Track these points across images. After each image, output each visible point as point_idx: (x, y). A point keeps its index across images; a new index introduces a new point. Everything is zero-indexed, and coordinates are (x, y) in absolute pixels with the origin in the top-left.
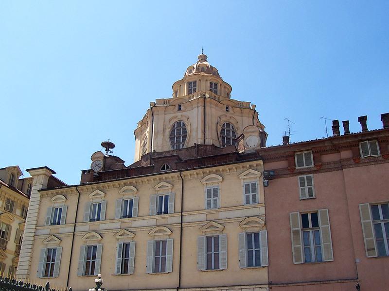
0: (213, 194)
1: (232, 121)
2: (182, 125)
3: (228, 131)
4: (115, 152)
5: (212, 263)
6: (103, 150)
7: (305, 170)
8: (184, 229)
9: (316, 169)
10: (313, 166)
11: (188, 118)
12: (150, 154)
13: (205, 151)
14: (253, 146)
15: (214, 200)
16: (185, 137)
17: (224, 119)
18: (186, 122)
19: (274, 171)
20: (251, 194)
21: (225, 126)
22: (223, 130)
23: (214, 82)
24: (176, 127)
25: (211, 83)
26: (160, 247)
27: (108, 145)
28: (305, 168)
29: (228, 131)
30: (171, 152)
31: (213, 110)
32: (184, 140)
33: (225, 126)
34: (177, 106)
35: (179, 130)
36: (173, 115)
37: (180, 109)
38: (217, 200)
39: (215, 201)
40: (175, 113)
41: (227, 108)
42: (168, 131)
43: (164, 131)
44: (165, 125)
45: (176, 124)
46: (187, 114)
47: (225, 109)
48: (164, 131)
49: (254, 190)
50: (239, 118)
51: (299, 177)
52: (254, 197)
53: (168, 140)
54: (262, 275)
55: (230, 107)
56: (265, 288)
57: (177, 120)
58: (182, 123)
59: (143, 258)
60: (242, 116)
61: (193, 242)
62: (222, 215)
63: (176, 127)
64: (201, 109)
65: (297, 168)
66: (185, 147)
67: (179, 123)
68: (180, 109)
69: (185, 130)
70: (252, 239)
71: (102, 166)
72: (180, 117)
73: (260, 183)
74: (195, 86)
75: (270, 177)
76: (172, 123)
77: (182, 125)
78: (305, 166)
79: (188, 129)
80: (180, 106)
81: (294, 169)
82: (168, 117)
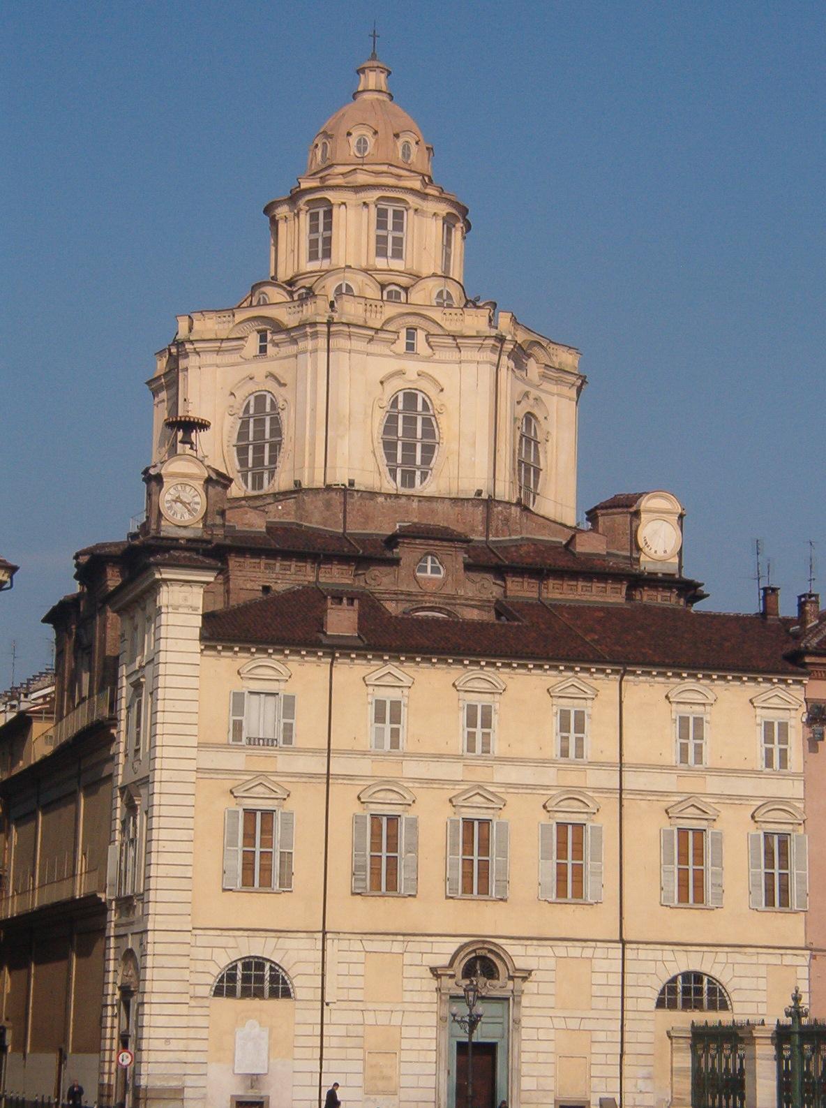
0: (691, 728)
5: (692, 889)
8: (625, 803)
13: (507, 520)
14: (660, 554)
15: (696, 745)
18: (436, 400)
20: (776, 748)
26: (569, 840)
34: (403, 333)
36: (394, 365)
37: (410, 347)
40: (398, 356)
42: (379, 419)
45: (401, 399)
49: (784, 738)
52: (783, 753)
54: (791, 928)
56: (803, 956)
57: (396, 385)
59: (526, 859)
61: (648, 835)
62: (714, 785)
64: (487, 372)
67: (410, 398)
68: (410, 347)
70: (776, 850)
71: (201, 508)
72: (412, 374)
73: (796, 720)
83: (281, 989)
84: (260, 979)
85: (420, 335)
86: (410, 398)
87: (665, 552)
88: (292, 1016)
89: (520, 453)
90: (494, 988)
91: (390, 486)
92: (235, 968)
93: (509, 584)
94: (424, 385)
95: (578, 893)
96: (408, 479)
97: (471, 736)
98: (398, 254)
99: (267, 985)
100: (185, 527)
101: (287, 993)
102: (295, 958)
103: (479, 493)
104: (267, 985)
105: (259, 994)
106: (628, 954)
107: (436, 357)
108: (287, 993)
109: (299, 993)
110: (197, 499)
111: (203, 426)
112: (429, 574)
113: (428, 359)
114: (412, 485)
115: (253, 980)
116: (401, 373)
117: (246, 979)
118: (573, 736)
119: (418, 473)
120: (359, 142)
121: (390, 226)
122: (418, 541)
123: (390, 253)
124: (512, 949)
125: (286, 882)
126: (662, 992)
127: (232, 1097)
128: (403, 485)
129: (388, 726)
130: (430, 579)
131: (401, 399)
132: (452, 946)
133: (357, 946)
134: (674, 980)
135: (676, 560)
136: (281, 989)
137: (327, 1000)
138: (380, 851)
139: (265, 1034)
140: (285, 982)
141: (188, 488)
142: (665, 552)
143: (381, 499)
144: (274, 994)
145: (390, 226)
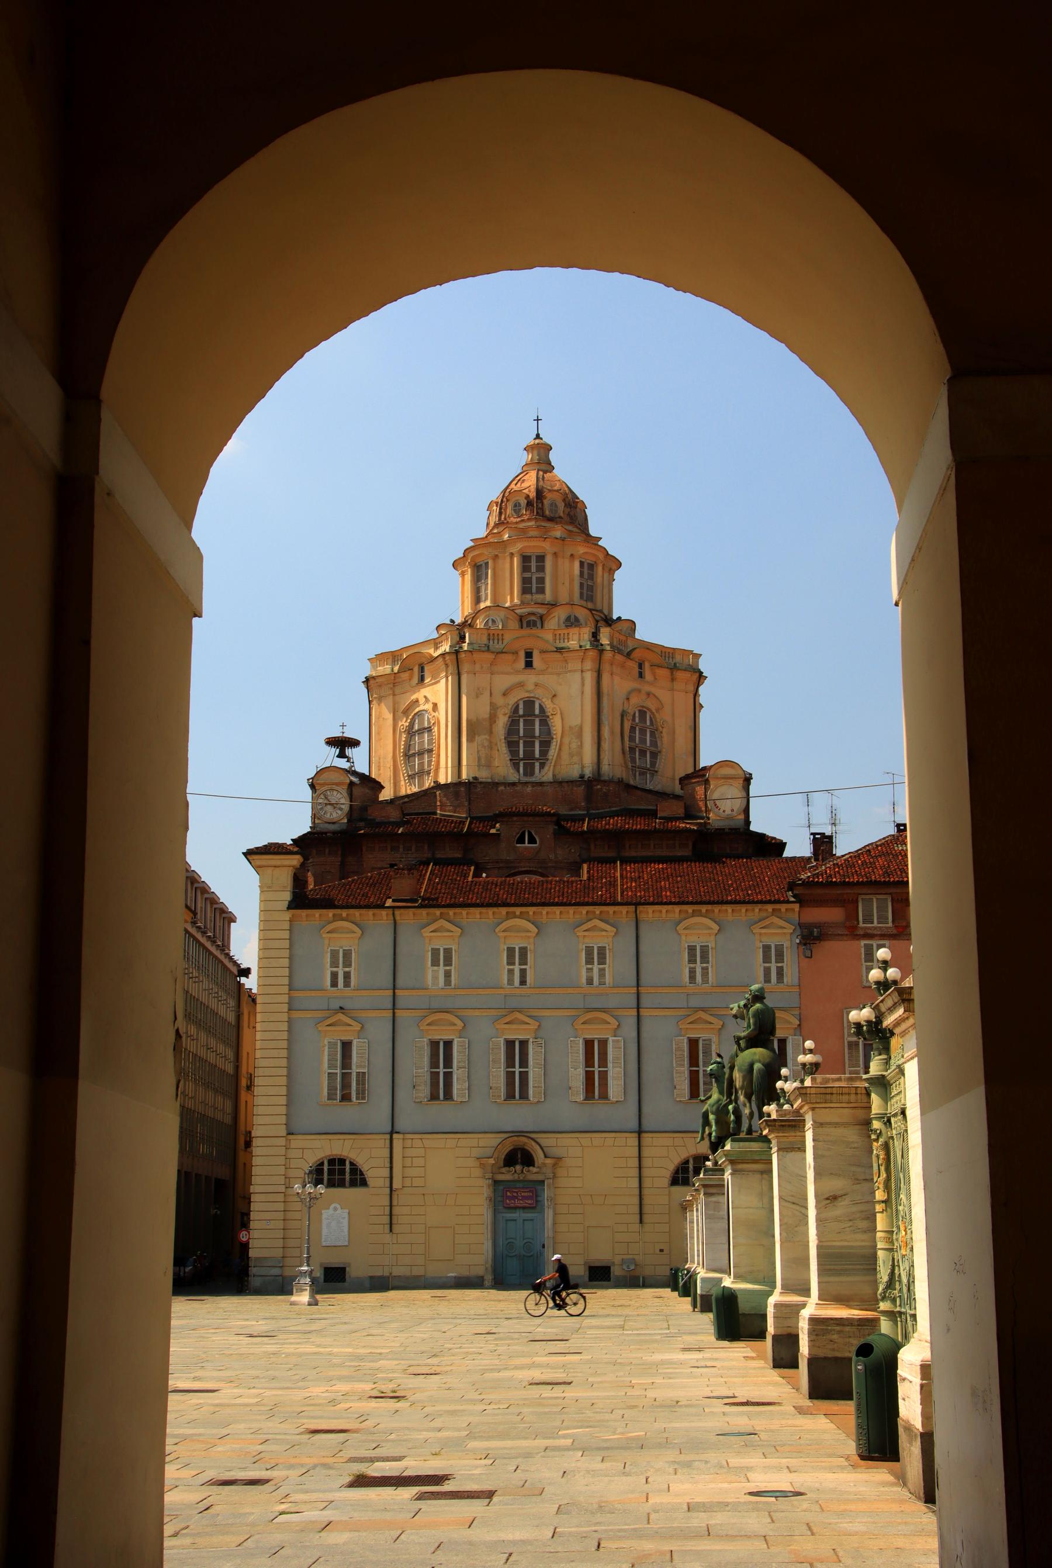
0: (697, 954)
1: (651, 704)
2: (537, 712)
3: (643, 732)
4: (360, 760)
6: (329, 757)
7: (875, 932)
9: (895, 932)
10: (890, 924)
11: (554, 696)
12: (471, 785)
14: (728, 812)
15: (703, 968)
16: (546, 744)
17: (635, 700)
18: (549, 706)
19: (819, 926)
21: (637, 720)
22: (633, 729)
23: (590, 559)
24: (521, 712)
25: (582, 564)
27: (342, 744)
28: (875, 928)
29: (643, 732)
30: (519, 788)
31: (617, 680)
32: (544, 753)
33: (637, 720)
35: (529, 723)
37: (529, 664)
38: (707, 968)
39: (705, 970)
40: (517, 672)
41: (640, 666)
42: (502, 721)
43: (493, 718)
44: (493, 706)
45: (521, 706)
46: (550, 680)
47: (637, 670)
48: (493, 718)
49: (780, 957)
50: (663, 695)
51: (863, 943)
53: (503, 748)
55: (647, 665)
57: (518, 695)
58: (537, 706)
60: (672, 690)
63: (521, 712)
64: (589, 678)
65: (861, 925)
66: (546, 775)
67: (529, 704)
68: (529, 664)
69: (545, 722)
72: (531, 687)
74: (541, 569)
75: (811, 937)
76: (512, 700)
77: (537, 712)
78: (875, 924)
79: (557, 725)
80: (529, 655)
81: (855, 928)
82: (503, 682)
83: (358, 1179)
84: (342, 1172)
85: (536, 654)
86: (529, 704)
87: (732, 810)
88: (368, 1200)
89: (632, 739)
90: (532, 1174)
91: (513, 776)
92: (322, 1164)
93: (592, 847)
94: (539, 693)
95: (524, 1096)
96: (529, 771)
97: (511, 972)
98: (541, 590)
99: (347, 1177)
100: (334, 823)
101: (364, 1183)
102: (368, 1156)
103: (582, 776)
104: (347, 1177)
105: (341, 1184)
106: (644, 1142)
107: (550, 670)
108: (364, 1183)
109: (370, 1182)
110: (343, 801)
111: (355, 743)
112: (527, 844)
113: (542, 672)
114: (532, 774)
115: (338, 1173)
116: (521, 685)
117: (331, 1172)
118: (596, 968)
119: (537, 765)
120: (515, 506)
121: (533, 569)
122: (515, 819)
123: (534, 590)
124: (547, 1140)
125: (361, 1094)
126: (677, 1172)
127: (349, 1265)
128: (525, 774)
129: (442, 969)
130: (526, 848)
131: (521, 706)
132: (493, 1140)
133: (418, 1143)
134: (687, 1162)
135: (742, 817)
136: (358, 1179)
137: (395, 1186)
138: (514, 1067)
139: (346, 1215)
140: (362, 1174)
141: (335, 793)
142: (732, 810)
143: (501, 788)
144: (353, 1184)
145: (533, 569)
